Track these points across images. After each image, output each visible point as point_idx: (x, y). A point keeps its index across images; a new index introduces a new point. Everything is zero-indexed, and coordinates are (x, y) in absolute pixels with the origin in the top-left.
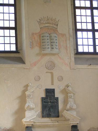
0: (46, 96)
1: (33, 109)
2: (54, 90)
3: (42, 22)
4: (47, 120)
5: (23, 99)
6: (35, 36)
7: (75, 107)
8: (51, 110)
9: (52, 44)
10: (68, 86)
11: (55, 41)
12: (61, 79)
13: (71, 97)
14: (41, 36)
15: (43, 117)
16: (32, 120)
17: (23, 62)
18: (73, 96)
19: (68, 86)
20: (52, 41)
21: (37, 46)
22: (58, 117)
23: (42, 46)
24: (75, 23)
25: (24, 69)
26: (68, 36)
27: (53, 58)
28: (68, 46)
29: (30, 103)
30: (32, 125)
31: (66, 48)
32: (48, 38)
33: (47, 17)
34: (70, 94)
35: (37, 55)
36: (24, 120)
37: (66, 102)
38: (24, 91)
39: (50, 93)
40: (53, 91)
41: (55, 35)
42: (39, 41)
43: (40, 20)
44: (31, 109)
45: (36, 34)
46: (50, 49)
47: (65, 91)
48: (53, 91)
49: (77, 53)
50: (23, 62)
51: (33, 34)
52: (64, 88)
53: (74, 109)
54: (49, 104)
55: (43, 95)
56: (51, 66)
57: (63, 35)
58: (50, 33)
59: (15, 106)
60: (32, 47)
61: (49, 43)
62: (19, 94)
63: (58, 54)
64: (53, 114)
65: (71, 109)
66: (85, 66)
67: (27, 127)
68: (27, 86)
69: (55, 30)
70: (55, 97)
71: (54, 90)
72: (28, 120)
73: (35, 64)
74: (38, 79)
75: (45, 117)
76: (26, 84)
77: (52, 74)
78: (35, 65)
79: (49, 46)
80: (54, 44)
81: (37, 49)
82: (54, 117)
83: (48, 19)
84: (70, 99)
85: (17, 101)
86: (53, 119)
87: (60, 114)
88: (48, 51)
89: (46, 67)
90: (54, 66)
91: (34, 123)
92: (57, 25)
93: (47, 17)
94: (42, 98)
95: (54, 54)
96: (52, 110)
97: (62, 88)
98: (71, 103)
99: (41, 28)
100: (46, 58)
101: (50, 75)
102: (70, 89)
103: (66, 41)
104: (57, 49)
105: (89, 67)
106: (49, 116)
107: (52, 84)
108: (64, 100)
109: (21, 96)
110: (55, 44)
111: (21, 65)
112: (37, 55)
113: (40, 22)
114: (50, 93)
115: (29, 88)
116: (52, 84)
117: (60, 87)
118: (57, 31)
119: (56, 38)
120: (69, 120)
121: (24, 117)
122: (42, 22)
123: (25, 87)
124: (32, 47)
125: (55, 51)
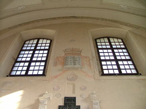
0: (65, 104)
2: (75, 98)
9: (75, 61)
11: (78, 60)
21: (60, 64)
24: (99, 56)
26: (91, 57)
34: (95, 101)
40: (74, 99)
45: (60, 57)
48: (74, 99)
51: (57, 57)
55: (62, 103)
60: (55, 64)
62: (33, 102)
70: (76, 105)
71: (75, 98)
78: (56, 78)
89: (67, 79)
90: (77, 78)
92: (81, 52)
102: (95, 96)
103: (89, 61)
107: (74, 92)
109: (34, 104)
117: (83, 96)
125: (77, 66)
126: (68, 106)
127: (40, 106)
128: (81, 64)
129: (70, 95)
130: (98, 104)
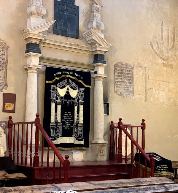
8: (68, 25)
13: (97, 10)
18: (100, 9)
54: (66, 15)
64: (69, 32)
70: (75, 5)
75: (58, 34)
82: (71, 36)
84: (96, 13)
96: (68, 24)
106: (64, 33)
130: (100, 12)
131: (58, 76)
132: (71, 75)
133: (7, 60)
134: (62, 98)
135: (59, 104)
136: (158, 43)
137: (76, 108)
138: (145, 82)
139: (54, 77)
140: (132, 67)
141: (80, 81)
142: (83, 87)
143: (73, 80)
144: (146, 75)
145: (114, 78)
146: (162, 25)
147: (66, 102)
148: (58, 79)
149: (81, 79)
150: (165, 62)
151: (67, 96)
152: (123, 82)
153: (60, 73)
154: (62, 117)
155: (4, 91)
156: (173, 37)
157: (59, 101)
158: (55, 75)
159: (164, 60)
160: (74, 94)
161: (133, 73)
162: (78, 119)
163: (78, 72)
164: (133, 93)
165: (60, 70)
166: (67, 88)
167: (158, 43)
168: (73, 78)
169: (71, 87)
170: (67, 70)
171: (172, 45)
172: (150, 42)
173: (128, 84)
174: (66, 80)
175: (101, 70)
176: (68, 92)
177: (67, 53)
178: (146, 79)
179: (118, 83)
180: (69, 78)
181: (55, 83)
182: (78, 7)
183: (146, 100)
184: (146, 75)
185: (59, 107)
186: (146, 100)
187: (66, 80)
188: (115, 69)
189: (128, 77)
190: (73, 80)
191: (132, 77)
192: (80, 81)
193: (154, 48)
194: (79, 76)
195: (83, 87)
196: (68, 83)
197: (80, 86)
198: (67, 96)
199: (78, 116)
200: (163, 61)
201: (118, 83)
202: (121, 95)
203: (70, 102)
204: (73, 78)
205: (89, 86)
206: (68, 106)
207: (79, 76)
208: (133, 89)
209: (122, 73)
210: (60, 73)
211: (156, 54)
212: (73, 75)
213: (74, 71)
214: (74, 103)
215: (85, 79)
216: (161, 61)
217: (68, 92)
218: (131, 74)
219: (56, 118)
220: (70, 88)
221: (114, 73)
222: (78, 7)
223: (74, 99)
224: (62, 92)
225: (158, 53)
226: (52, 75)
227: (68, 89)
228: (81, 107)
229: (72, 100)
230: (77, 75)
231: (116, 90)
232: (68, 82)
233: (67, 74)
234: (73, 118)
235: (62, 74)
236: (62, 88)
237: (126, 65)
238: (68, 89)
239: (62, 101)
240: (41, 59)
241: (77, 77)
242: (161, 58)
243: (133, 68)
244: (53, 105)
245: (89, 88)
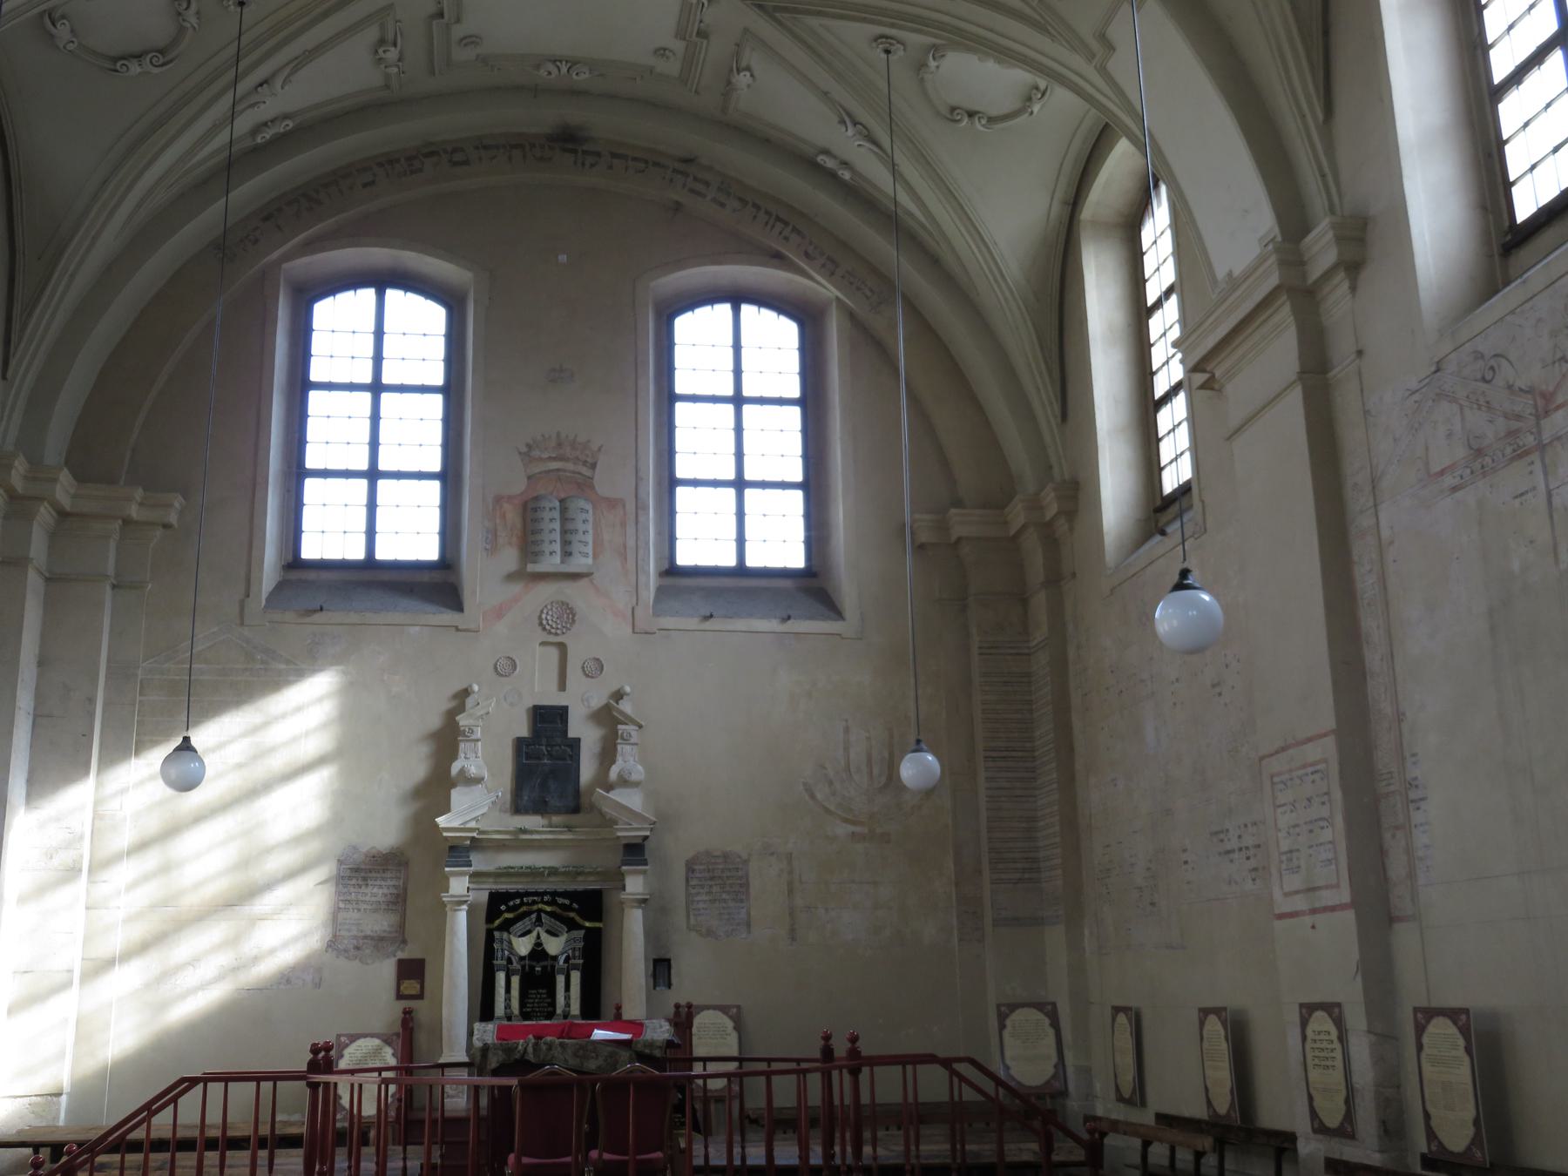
1: (478, 780)
3: (536, 453)
4: (533, 822)
5: (447, 740)
6: (506, 506)
7: (638, 772)
10: (619, 695)
11: (581, 527)
12: (595, 668)
13: (626, 741)
14: (530, 510)
15: (518, 809)
16: (473, 825)
17: (458, 606)
19: (619, 695)
20: (570, 526)
22: (576, 810)
23: (529, 546)
25: (457, 629)
26: (631, 507)
27: (569, 590)
28: (631, 543)
29: (469, 761)
30: (473, 839)
31: (622, 554)
32: (556, 514)
33: (558, 434)
35: (511, 577)
36: (442, 821)
37: (608, 754)
38: (451, 716)
39: (549, 720)
40: (561, 714)
41: (582, 503)
42: (519, 526)
43: (529, 446)
44: (470, 781)
45: (510, 498)
46: (557, 559)
47: (608, 718)
48: (561, 714)
49: (672, 571)
50: (458, 606)
51: (498, 500)
52: (603, 702)
53: (636, 784)
55: (523, 731)
56: (558, 627)
57: (613, 503)
58: (563, 496)
59: (418, 768)
60: (492, 547)
61: (557, 536)
62: (434, 721)
63: (588, 575)
64: (554, 802)
65: (624, 782)
66: (693, 623)
67: (452, 848)
68: (466, 693)
69: (584, 486)
72: (455, 824)
73: (499, 613)
74: (506, 668)
76: (458, 687)
77: (562, 647)
79: (557, 547)
80: (575, 538)
81: (509, 558)
82: (558, 812)
83: (560, 445)
85: (424, 750)
86: (556, 819)
87: (584, 800)
88: (552, 562)
89: (541, 624)
91: (481, 832)
92: (593, 466)
93: (558, 434)
94: (520, 743)
95: (575, 576)
97: (597, 702)
98: (628, 761)
99: (529, 478)
100: (546, 592)
101: (554, 653)
102: (626, 706)
103: (623, 524)
104: (586, 555)
105: (708, 625)
106: (539, 808)
107: (562, 686)
108: (603, 749)
110: (580, 536)
111: (448, 617)
112: (511, 577)
113: (527, 455)
114: (549, 720)
115: (470, 702)
116: (562, 686)
118: (592, 487)
119: (584, 516)
120: (614, 822)
121: (446, 809)
122: (536, 453)
123: (455, 696)
124: (492, 547)
126: (544, 741)
127: (462, 745)
128: (589, 549)
129: (553, 699)
131: (509, 910)
132: (547, 903)
133: (405, 890)
134: (522, 958)
135: (515, 972)
136: (831, 783)
137: (560, 979)
138: (791, 891)
139: (502, 913)
140: (745, 856)
141: (572, 915)
142: (581, 927)
143: (551, 914)
144: (791, 872)
145: (688, 895)
146: (847, 730)
147: (532, 968)
148: (507, 915)
149: (573, 910)
150: (858, 829)
151: (538, 953)
152: (713, 901)
153: (518, 901)
154: (522, 1004)
155: (401, 955)
156: (886, 755)
157: (516, 965)
158: (503, 908)
159: (854, 823)
160: (554, 946)
161: (747, 876)
162: (568, 1005)
163: (565, 894)
164: (749, 925)
165: (518, 895)
166: (534, 934)
167: (831, 783)
168: (548, 909)
169: (548, 932)
170: (528, 894)
171: (883, 780)
172: (805, 784)
173: (731, 904)
174: (534, 916)
175: (635, 885)
176: (538, 944)
177: (544, 851)
178: (790, 885)
179: (701, 905)
180: (540, 911)
181: (506, 926)
182: (579, 740)
183: (793, 939)
184: (791, 872)
185: (515, 980)
186: (793, 939)
187: (534, 916)
188: (690, 868)
189: (731, 885)
190: (551, 914)
191: (746, 885)
192: (572, 915)
193: (819, 796)
194: (567, 902)
195: (581, 927)
196: (539, 922)
197: (572, 925)
198: (538, 953)
199: (567, 998)
200: (851, 828)
201: (701, 905)
202: (710, 933)
203: (544, 968)
204: (548, 909)
205: (597, 925)
206: (538, 977)
207: (567, 902)
208: (748, 914)
209: (712, 878)
210: (518, 901)
211: (827, 811)
212: (552, 903)
213: (554, 894)
214: (553, 967)
215: (585, 909)
216: (842, 830)
217: (538, 944)
218: (740, 878)
219: (508, 1006)
220: (544, 936)
221: (687, 880)
222: (579, 740)
223: (555, 958)
224: (523, 946)
225: (832, 808)
226: (502, 910)
227: (538, 937)
228: (576, 977)
229: (548, 963)
230: (560, 900)
231: (692, 921)
232: (539, 919)
233: (534, 902)
234: (553, 1004)
235: (522, 904)
236: (523, 935)
237: (726, 856)
238: (538, 937)
239: (523, 967)
240: (476, 876)
241: (563, 907)
242: (846, 821)
243: (746, 862)
244: (501, 977)
245: (599, 930)
